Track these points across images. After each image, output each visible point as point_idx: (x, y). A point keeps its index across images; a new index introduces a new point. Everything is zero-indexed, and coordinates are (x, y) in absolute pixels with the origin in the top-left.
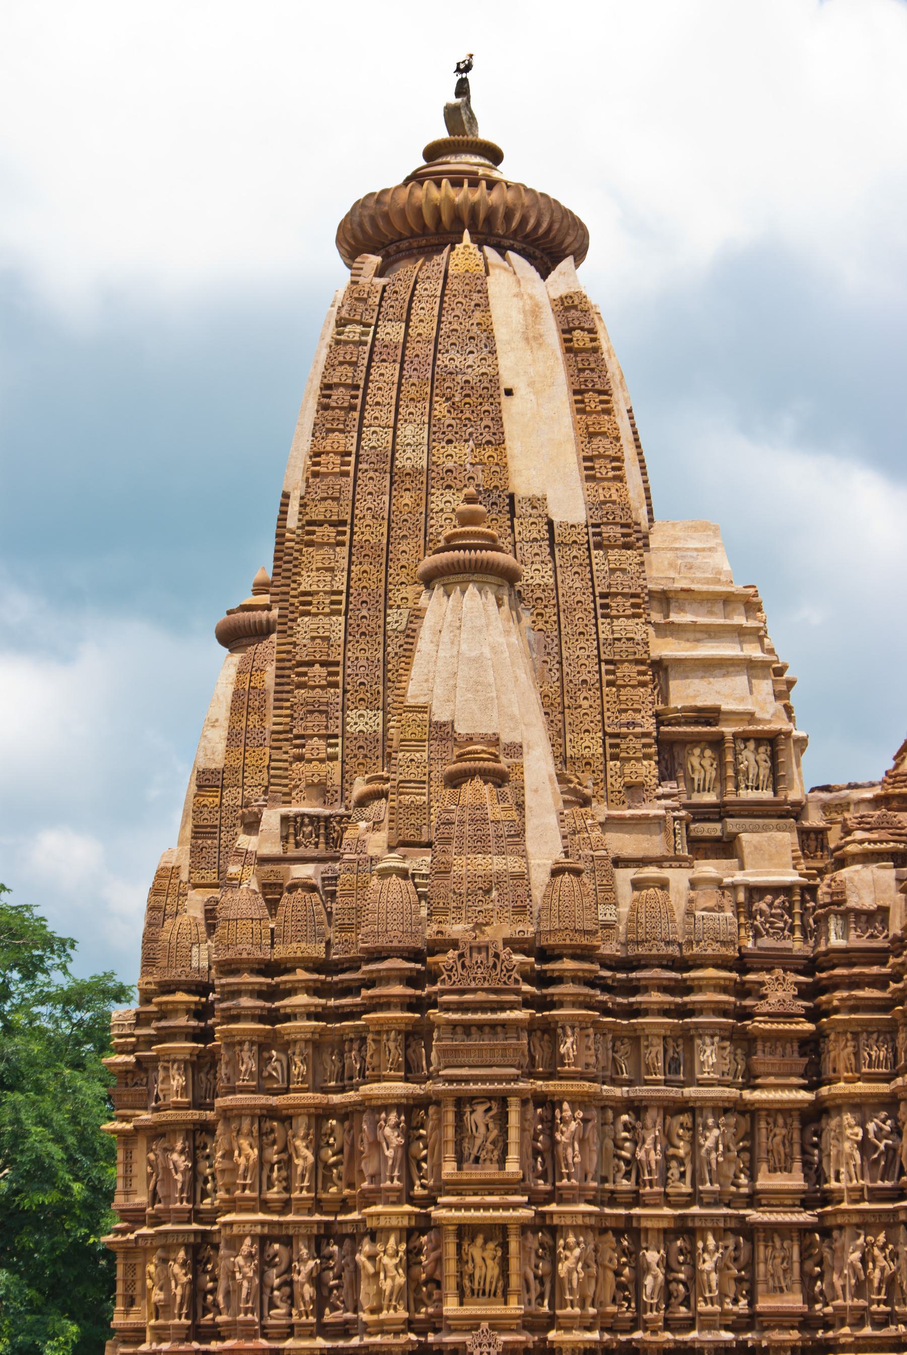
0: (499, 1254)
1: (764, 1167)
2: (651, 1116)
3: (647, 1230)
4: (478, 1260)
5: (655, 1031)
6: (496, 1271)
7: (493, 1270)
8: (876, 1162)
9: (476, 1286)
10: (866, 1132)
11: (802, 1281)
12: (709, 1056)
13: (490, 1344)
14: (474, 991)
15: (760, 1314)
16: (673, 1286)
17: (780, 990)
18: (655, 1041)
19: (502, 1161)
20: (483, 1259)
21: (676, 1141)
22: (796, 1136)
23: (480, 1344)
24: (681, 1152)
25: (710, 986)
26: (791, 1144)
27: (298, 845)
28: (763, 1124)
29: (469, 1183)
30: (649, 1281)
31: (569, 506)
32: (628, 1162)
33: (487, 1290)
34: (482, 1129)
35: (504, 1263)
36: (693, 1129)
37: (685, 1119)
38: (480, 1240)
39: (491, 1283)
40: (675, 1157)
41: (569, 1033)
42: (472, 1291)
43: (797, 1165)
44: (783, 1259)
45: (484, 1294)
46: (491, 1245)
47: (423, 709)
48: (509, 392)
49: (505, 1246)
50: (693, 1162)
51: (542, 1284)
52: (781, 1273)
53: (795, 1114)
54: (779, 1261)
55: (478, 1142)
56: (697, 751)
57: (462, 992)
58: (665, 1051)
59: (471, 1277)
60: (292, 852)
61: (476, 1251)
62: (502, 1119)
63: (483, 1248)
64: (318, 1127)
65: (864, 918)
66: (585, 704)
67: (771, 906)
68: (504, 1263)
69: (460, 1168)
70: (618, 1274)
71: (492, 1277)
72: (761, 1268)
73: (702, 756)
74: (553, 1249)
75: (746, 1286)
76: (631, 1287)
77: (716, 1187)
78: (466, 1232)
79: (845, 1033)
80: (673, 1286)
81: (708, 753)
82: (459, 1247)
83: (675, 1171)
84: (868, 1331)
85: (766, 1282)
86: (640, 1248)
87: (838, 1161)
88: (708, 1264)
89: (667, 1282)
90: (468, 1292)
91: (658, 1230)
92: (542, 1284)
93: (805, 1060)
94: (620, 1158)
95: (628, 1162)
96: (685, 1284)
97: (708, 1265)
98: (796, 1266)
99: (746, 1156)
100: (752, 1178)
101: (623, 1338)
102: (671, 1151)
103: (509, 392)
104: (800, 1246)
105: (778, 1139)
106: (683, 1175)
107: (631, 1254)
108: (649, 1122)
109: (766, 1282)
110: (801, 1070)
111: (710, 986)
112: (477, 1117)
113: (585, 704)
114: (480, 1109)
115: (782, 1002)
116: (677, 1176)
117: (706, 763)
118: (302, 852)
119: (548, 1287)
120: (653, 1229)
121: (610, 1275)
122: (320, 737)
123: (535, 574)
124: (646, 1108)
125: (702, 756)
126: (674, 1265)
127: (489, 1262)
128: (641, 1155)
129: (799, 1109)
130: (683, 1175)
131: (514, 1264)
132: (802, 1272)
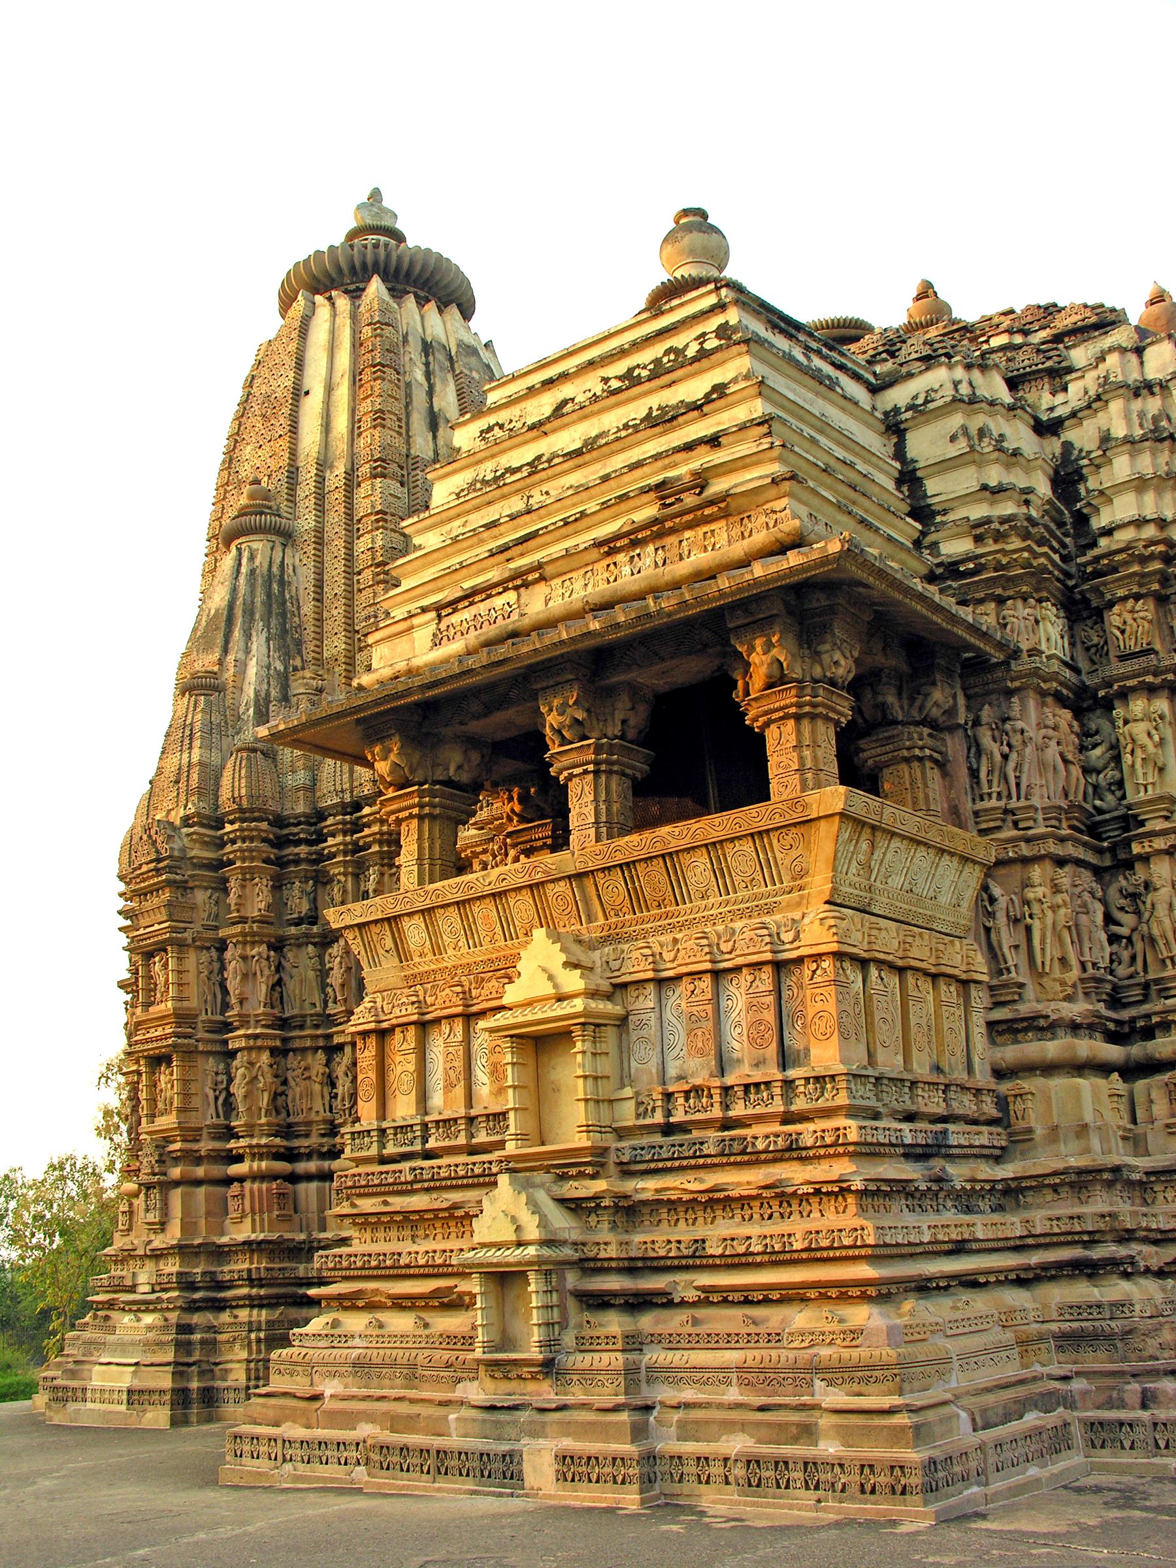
66: (335, 612)
113: (335, 612)
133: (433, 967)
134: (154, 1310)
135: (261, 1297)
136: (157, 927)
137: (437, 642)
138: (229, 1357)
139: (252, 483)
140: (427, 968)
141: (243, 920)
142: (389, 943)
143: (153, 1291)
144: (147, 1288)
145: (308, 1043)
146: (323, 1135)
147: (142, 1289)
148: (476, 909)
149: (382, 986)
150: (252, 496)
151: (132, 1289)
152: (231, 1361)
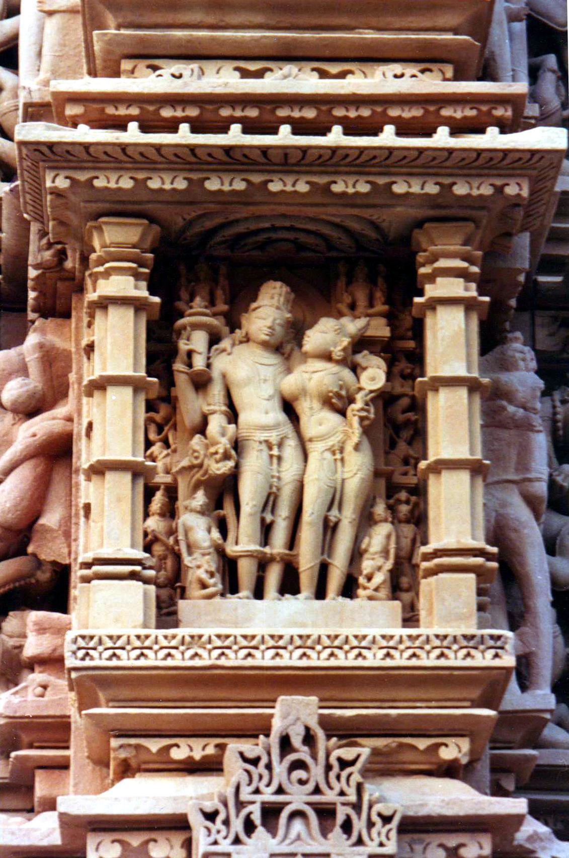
0: (374, 375)
4: (260, 414)
6: (357, 469)
7: (336, 460)
9: (244, 542)
13: (326, 813)
20: (289, 408)
23: (271, 813)
33: (307, 562)
35: (397, 426)
38: (268, 310)
39: (329, 529)
42: (228, 569)
45: (290, 585)
46: (325, 333)
49: (404, 351)
59: (223, 492)
61: (248, 372)
63: (286, 345)
68: (397, 426)
69: (166, 614)
71: (335, 500)
82: (161, 350)
90: (200, 566)
127: (318, 421)
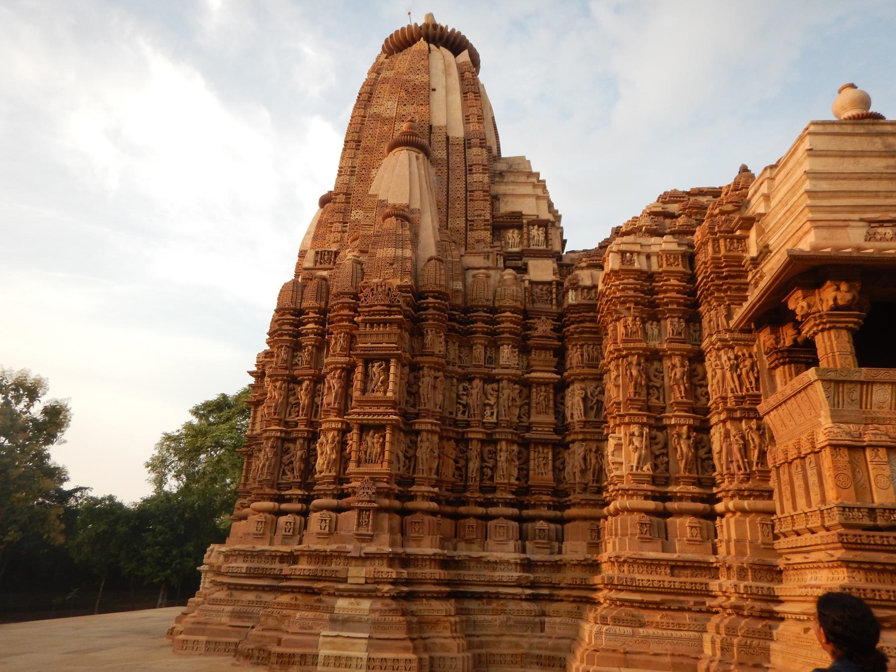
1: (533, 411)
2: (477, 383)
3: (472, 439)
5: (479, 341)
8: (592, 408)
10: (586, 394)
11: (554, 471)
12: (506, 354)
14: (376, 305)
15: (531, 486)
16: (485, 470)
17: (543, 327)
18: (479, 346)
19: (385, 392)
21: (490, 397)
22: (551, 396)
24: (492, 402)
25: (508, 321)
26: (549, 401)
27: (321, 263)
28: (534, 390)
29: (367, 401)
30: (471, 465)
31: (458, 131)
32: (465, 406)
34: (377, 375)
35: (383, 445)
36: (498, 391)
37: (495, 386)
38: (371, 433)
40: (488, 404)
41: (429, 332)
43: (551, 412)
44: (544, 458)
47: (375, 196)
48: (434, 90)
50: (497, 407)
51: (410, 461)
52: (542, 466)
53: (551, 386)
54: (541, 459)
55: (374, 382)
56: (511, 231)
57: (371, 306)
58: (486, 353)
60: (318, 266)
62: (387, 370)
63: (373, 437)
64: (315, 386)
65: (586, 290)
66: (458, 206)
67: (541, 290)
70: (456, 462)
72: (532, 462)
73: (513, 233)
74: (416, 442)
75: (525, 472)
76: (464, 470)
77: (508, 418)
78: (364, 428)
79: (576, 345)
80: (485, 470)
81: (516, 231)
83: (488, 411)
84: (588, 496)
85: (534, 470)
86: (467, 448)
87: (572, 408)
88: (503, 457)
89: (482, 468)
90: (363, 460)
91: (478, 440)
92: (410, 461)
93: (557, 359)
94: (460, 404)
95: (465, 406)
96: (491, 469)
97: (503, 459)
98: (550, 463)
99: (526, 407)
100: (529, 418)
101: (458, 495)
102: (487, 401)
103: (434, 90)
104: (553, 452)
105: (542, 398)
106: (492, 414)
107: (465, 452)
108: (474, 386)
109: (534, 470)
110: (554, 364)
111: (508, 321)
112: (375, 369)
113: (458, 206)
114: (376, 365)
115: (544, 331)
116: (489, 414)
117: (515, 236)
118: (323, 266)
119: (413, 463)
120: (475, 439)
121: (451, 462)
122: (340, 222)
123: (440, 153)
124: (473, 379)
125: (513, 233)
126: (486, 459)
128: (470, 402)
129: (553, 383)
130: (492, 414)
131: (387, 445)
132: (554, 466)
133: (889, 416)
134: (369, 597)
135: (441, 592)
136: (384, 345)
137: (870, 238)
138: (432, 634)
139: (411, 121)
140: (883, 416)
141: (432, 354)
142: (856, 395)
143: (366, 583)
144: (363, 581)
145: (451, 434)
146: (447, 490)
147: (349, 581)
148: (874, 387)
149: (844, 419)
150: (410, 127)
151: (345, 580)
152: (438, 637)
